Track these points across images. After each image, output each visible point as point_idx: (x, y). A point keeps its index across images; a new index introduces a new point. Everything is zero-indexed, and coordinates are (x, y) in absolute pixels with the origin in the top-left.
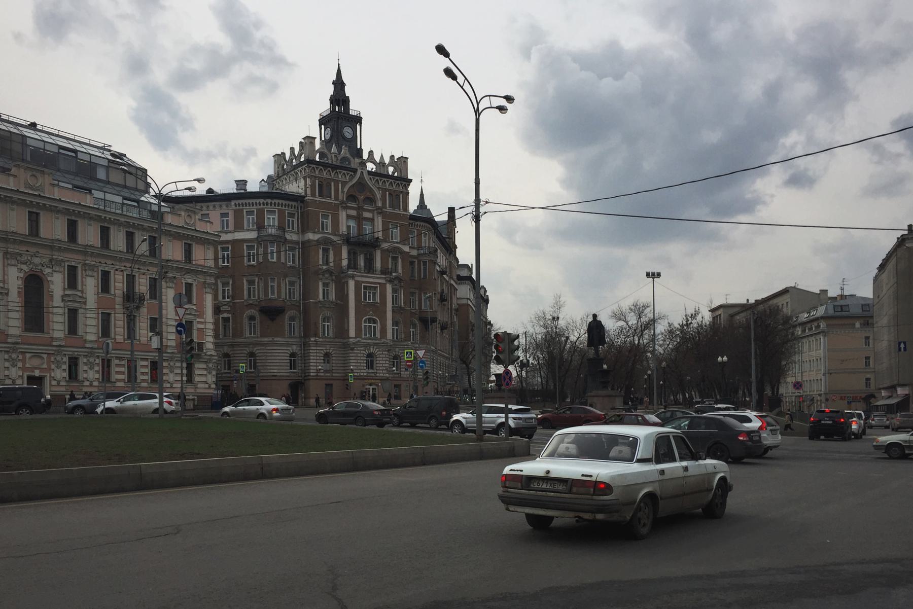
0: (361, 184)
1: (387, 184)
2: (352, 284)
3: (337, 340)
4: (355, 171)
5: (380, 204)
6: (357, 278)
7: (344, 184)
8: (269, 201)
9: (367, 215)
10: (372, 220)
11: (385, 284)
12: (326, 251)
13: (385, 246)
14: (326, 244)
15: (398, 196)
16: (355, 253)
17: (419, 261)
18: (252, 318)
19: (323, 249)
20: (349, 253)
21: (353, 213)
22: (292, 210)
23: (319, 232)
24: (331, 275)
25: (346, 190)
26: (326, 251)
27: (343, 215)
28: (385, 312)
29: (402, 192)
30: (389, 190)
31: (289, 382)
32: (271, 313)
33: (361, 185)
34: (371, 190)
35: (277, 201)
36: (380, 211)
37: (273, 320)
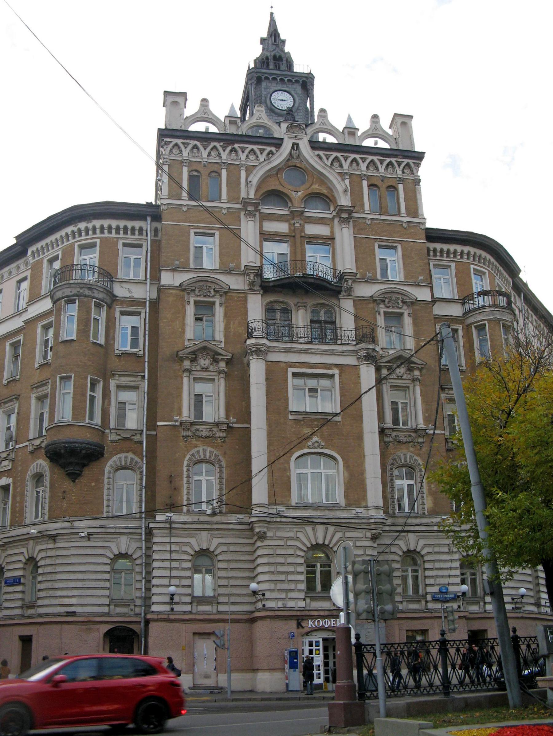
0: (294, 165)
1: (363, 166)
2: (257, 370)
3: (233, 518)
4: (278, 143)
5: (344, 201)
6: (273, 357)
7: (250, 170)
8: (82, 225)
9: (312, 229)
10: (329, 241)
11: (356, 367)
12: (204, 309)
13: (365, 291)
14: (205, 294)
15: (393, 188)
16: (286, 311)
17: (468, 328)
18: (39, 478)
19: (197, 304)
20: (269, 310)
21: (283, 227)
22: (135, 239)
23: (184, 268)
24: (215, 361)
25: (255, 179)
26: (204, 309)
27: (249, 229)
28: (360, 437)
29: (401, 180)
30: (368, 178)
31: (105, 628)
32: (75, 458)
33: (294, 165)
34: (322, 179)
35: (97, 223)
36: (346, 215)
37: (74, 476)
